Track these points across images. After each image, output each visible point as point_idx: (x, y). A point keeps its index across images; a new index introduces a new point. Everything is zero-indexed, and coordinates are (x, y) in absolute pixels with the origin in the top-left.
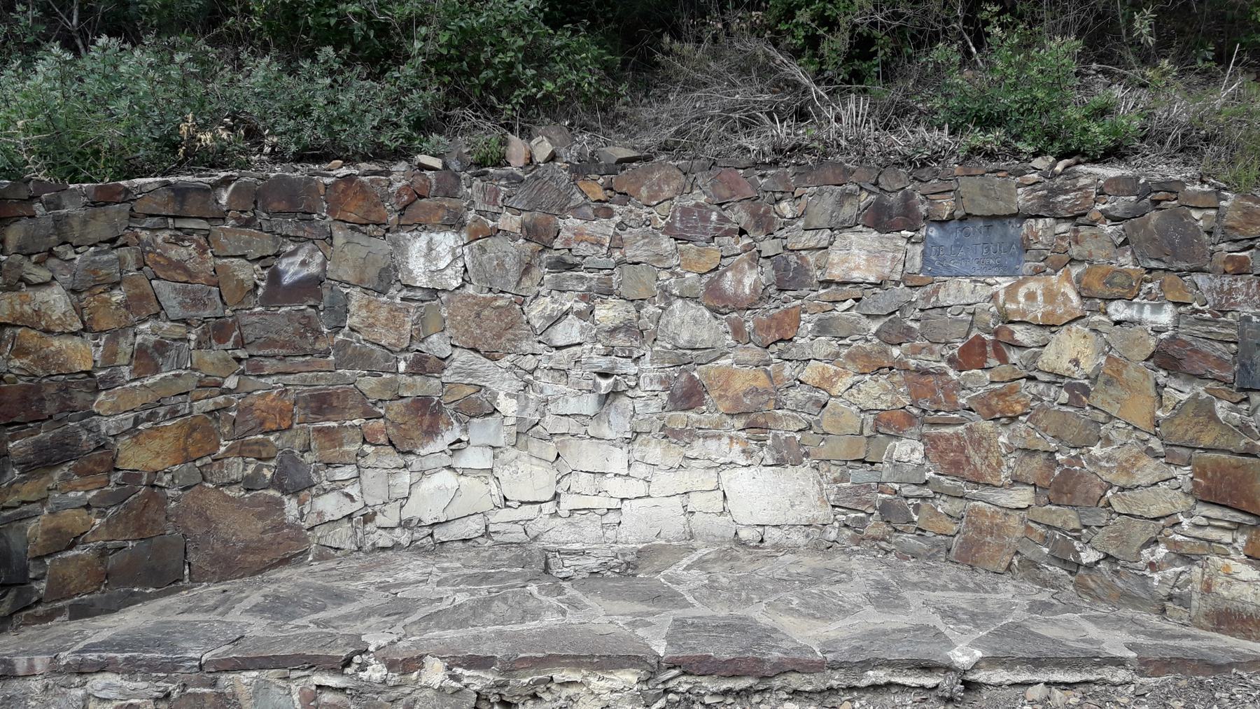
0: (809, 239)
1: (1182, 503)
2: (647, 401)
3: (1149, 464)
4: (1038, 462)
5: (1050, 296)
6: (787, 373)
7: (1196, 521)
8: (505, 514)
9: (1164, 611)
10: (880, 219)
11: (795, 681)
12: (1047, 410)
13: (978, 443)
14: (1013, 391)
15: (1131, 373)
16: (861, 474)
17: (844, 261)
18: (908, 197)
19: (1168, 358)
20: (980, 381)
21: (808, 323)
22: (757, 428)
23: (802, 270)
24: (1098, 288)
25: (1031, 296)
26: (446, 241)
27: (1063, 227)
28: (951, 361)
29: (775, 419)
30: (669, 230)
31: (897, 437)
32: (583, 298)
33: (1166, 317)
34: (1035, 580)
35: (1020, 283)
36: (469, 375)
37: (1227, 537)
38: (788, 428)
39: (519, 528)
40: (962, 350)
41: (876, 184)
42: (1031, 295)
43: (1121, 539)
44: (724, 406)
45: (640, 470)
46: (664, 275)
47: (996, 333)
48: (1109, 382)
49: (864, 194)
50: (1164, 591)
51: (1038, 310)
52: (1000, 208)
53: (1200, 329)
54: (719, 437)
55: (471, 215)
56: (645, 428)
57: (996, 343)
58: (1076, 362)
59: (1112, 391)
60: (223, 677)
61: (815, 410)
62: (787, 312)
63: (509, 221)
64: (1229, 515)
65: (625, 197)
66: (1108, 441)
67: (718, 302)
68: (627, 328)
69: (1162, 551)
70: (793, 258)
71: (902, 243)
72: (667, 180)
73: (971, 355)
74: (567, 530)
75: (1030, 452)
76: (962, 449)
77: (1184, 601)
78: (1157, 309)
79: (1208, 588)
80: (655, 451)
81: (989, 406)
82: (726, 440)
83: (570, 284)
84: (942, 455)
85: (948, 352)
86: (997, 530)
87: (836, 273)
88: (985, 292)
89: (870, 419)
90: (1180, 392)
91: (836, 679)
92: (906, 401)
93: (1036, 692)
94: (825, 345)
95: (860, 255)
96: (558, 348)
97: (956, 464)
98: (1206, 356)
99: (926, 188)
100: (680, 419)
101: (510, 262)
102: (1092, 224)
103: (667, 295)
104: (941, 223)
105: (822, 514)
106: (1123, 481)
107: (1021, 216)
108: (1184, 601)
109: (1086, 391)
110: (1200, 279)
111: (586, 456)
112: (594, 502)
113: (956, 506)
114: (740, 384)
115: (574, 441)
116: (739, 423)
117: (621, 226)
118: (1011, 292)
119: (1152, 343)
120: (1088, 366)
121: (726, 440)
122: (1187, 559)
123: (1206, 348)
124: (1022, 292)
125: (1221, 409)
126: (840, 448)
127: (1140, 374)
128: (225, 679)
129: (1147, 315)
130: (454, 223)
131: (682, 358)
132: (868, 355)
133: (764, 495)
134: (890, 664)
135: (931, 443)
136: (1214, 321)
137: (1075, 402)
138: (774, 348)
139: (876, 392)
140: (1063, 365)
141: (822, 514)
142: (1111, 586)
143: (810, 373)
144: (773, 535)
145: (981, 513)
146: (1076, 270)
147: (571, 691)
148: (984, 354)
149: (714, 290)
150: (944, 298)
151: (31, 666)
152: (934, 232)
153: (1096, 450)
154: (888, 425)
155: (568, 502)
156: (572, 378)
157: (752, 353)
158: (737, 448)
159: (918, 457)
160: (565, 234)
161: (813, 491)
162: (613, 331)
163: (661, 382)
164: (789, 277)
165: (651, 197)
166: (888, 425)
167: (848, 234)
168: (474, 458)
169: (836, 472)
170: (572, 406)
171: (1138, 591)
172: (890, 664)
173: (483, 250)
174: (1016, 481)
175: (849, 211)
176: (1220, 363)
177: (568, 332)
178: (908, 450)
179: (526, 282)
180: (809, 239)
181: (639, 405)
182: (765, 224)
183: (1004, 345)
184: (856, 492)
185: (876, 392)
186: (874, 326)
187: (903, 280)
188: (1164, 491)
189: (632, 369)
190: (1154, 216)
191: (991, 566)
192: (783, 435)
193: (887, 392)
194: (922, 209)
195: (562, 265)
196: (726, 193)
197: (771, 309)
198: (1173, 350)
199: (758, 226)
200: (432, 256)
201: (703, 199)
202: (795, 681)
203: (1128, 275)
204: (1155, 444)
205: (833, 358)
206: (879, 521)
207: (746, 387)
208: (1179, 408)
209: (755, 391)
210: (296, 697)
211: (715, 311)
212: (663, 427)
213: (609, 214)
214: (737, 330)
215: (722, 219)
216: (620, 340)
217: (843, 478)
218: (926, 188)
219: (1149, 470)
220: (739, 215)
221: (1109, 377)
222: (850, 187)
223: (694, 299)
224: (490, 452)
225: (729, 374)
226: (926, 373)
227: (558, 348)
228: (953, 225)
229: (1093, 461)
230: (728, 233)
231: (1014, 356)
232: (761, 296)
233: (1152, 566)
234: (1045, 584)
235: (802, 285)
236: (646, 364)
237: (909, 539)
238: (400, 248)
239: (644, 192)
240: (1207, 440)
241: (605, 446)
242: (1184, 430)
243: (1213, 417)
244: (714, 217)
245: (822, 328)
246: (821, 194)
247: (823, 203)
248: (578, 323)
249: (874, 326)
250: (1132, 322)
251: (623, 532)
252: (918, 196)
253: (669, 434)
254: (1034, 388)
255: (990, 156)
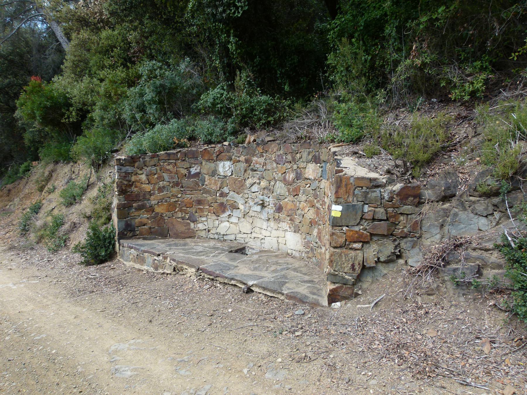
2: (270, 210)
8: (240, 235)
26: (228, 164)
30: (275, 161)
32: (259, 179)
54: (285, 222)
55: (233, 157)
72: (275, 146)
80: (272, 223)
83: (255, 175)
114: (289, 207)
115: (256, 218)
130: (230, 159)
131: (279, 198)
134: (237, 280)
158: (288, 226)
160: (254, 162)
168: (234, 220)
177: (255, 188)
179: (246, 174)
200: (224, 167)
215: (286, 158)
216: (266, 191)
230: (287, 162)
236: (271, 199)
238: (217, 165)
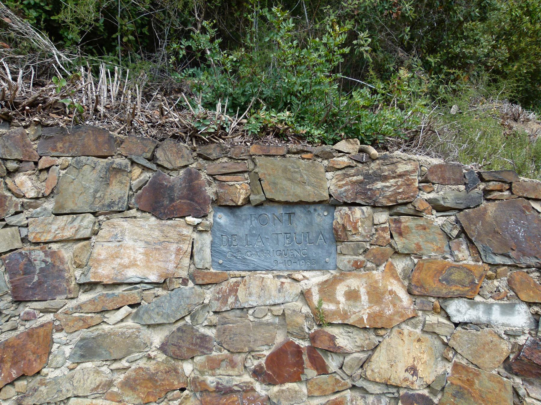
5: (376, 295)
10: (158, 202)
17: (114, 256)
18: (192, 177)
21: (64, 345)
24: (433, 285)
27: (382, 217)
28: (257, 373)
40: (271, 359)
41: (153, 159)
42: (357, 292)
47: (313, 338)
49: (137, 171)
51: (363, 310)
52: (307, 193)
57: (312, 350)
58: (413, 370)
62: (30, 334)
70: (38, 255)
71: (187, 232)
78: (508, 309)
85: (253, 364)
87: (104, 272)
99: (213, 167)
102: (417, 214)
107: (332, 203)
118: (327, 289)
119: (505, 347)
124: (341, 290)
129: (496, 316)
132: (152, 378)
140: (399, 375)
146: (400, 265)
148: (300, 364)
150: (248, 296)
152: (223, 219)
167: (117, 220)
175: (117, 191)
180: (62, 227)
186: (157, 338)
187: (192, 277)
194: (210, 191)
222: (119, 161)
228: (246, 211)
245: (87, 351)
246: (79, 167)
247: (83, 180)
250: (478, 325)
252: (204, 176)
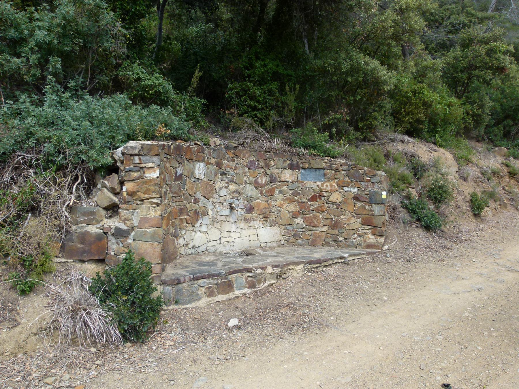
0: (277, 171)
1: (360, 225)
2: (240, 211)
3: (353, 219)
4: (329, 221)
5: (331, 186)
6: (272, 203)
7: (363, 229)
8: (210, 244)
9: (356, 247)
10: (292, 167)
11: (326, 263)
12: (331, 210)
13: (315, 218)
14: (323, 206)
15: (349, 201)
16: (289, 227)
17: (285, 176)
18: (298, 163)
19: (356, 198)
20: (316, 204)
21: (277, 191)
22: (266, 217)
23: (275, 178)
24: (341, 184)
25: (327, 186)
26: (202, 165)
27: (333, 172)
28: (309, 200)
29: (270, 215)
30: (247, 166)
31: (296, 218)
32: (227, 183)
33: (356, 190)
34: (328, 246)
35: (324, 183)
36: (204, 204)
37: (368, 231)
38: (273, 218)
39: (212, 248)
40: (311, 197)
41: (291, 159)
42: (327, 186)
43: (348, 234)
44: (258, 212)
45: (239, 230)
46: (245, 178)
47: (319, 194)
48: (345, 203)
49: (288, 161)
50: (356, 243)
51: (329, 189)
52: (320, 167)
53: (362, 192)
54: (257, 220)
55: (206, 159)
56: (240, 219)
57: (319, 196)
58: (337, 199)
59: (345, 205)
60: (229, 276)
61: (278, 212)
62: (272, 188)
63: (213, 161)
64: (369, 227)
65: (238, 157)
66: (345, 215)
67: (257, 185)
68: (237, 191)
69: (356, 235)
70: (274, 175)
71: (296, 173)
72: (247, 153)
73: (314, 198)
74: (223, 247)
75: (327, 219)
76: (312, 219)
77: (360, 245)
78: (354, 188)
79: (365, 241)
80: (242, 225)
81: (318, 210)
82: (258, 221)
83: (224, 179)
84: (307, 221)
85: (308, 198)
86: (320, 237)
87: (283, 179)
88: (316, 185)
89: (291, 214)
90: (359, 204)
91: (331, 262)
92: (299, 209)
93: (356, 260)
94: (281, 196)
95: (288, 175)
96: (221, 197)
97: (310, 223)
98: (364, 197)
99: (302, 161)
100: (249, 216)
101: (213, 172)
102: (339, 171)
103: (246, 183)
104: (305, 169)
105: (280, 238)
106: (348, 223)
107: (324, 169)
108: (360, 245)
109: (339, 205)
110: (362, 183)
111: (227, 227)
112: (228, 240)
113: (310, 233)
114: (262, 206)
115: (224, 223)
116: (261, 216)
117: (237, 164)
118: (322, 185)
119: (353, 195)
120: (340, 200)
121: (258, 221)
122: (360, 236)
123: (364, 196)
124: (325, 185)
125: (367, 207)
126: (284, 221)
127: (351, 201)
128: (230, 277)
129: (352, 190)
130: (203, 161)
131: (249, 199)
132: (290, 199)
133: (267, 234)
134: (337, 258)
135: (305, 219)
136: (365, 191)
137: (337, 208)
138: (269, 197)
139: (293, 208)
140: (335, 200)
141: (280, 238)
142: (345, 244)
143: (277, 203)
144: (269, 244)
145: (316, 233)
146: (336, 181)
147: (292, 271)
148: (317, 198)
149: (256, 182)
150: (307, 185)
151: (185, 280)
152: (303, 171)
153: (342, 217)
154: (295, 215)
155: (223, 240)
156: (224, 205)
157: (264, 198)
158: (261, 223)
159: (302, 222)
160: (225, 165)
161: (278, 232)
162: (233, 192)
163: (244, 206)
164: (273, 180)
165: (244, 157)
166: (295, 215)
167: (285, 170)
168: (204, 228)
169: (284, 227)
170: (223, 213)
171: (351, 244)
172: (337, 258)
173: (208, 168)
174: (324, 225)
175: (285, 165)
176: (366, 198)
177: (223, 192)
178: (299, 221)
179: (216, 178)
180: (277, 171)
181: (239, 212)
182: (268, 166)
183: (321, 196)
184: (287, 232)
185: (293, 208)
186: (291, 192)
187: (297, 181)
188: (356, 223)
189: (238, 203)
190: (352, 171)
191: (318, 245)
192: (271, 219)
193: (294, 207)
194: (301, 166)
195: (224, 174)
196: (260, 158)
197: (269, 187)
198: (358, 196)
199: (266, 166)
200: (200, 169)
201: (254, 159)
202: (326, 263)
203: (347, 181)
204: (354, 214)
205: (282, 200)
206: (294, 238)
207: (263, 207)
208: (359, 208)
209: (265, 208)
210: (244, 279)
211: (256, 188)
212: (244, 218)
213: (234, 161)
214: (261, 193)
215: (259, 164)
216: (235, 195)
217: (285, 229)
218: (302, 161)
219: (353, 220)
220: (262, 164)
221: (345, 202)
222: (286, 159)
223: (251, 184)
224: (206, 226)
225: (259, 204)
226: (303, 203)
227: (221, 197)
228: (307, 170)
229: (342, 219)
230: (259, 168)
231: (323, 198)
232: (266, 184)
233: (355, 239)
234: (331, 246)
235: (276, 182)
236: (240, 201)
237: (300, 241)
238: (194, 166)
239: (242, 156)
240: (364, 213)
241: (231, 224)
242: (360, 212)
243: (365, 209)
244: (257, 163)
245: (281, 192)
246: (279, 160)
247: (280, 162)
248: (226, 190)
249: (291, 192)
250: (349, 191)
251: (235, 247)
252: (300, 163)
253: (246, 220)
254: (327, 205)
255: (314, 155)
